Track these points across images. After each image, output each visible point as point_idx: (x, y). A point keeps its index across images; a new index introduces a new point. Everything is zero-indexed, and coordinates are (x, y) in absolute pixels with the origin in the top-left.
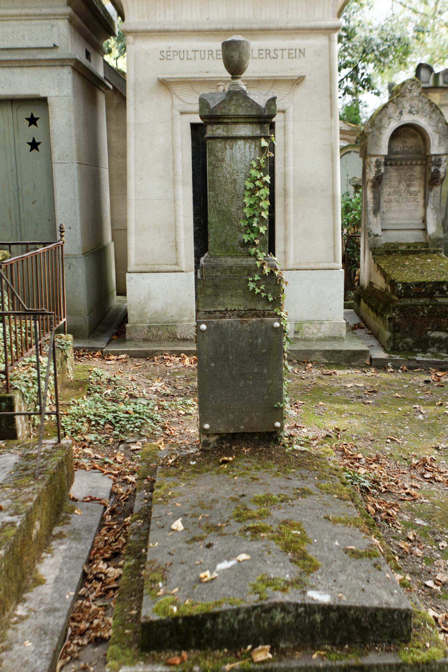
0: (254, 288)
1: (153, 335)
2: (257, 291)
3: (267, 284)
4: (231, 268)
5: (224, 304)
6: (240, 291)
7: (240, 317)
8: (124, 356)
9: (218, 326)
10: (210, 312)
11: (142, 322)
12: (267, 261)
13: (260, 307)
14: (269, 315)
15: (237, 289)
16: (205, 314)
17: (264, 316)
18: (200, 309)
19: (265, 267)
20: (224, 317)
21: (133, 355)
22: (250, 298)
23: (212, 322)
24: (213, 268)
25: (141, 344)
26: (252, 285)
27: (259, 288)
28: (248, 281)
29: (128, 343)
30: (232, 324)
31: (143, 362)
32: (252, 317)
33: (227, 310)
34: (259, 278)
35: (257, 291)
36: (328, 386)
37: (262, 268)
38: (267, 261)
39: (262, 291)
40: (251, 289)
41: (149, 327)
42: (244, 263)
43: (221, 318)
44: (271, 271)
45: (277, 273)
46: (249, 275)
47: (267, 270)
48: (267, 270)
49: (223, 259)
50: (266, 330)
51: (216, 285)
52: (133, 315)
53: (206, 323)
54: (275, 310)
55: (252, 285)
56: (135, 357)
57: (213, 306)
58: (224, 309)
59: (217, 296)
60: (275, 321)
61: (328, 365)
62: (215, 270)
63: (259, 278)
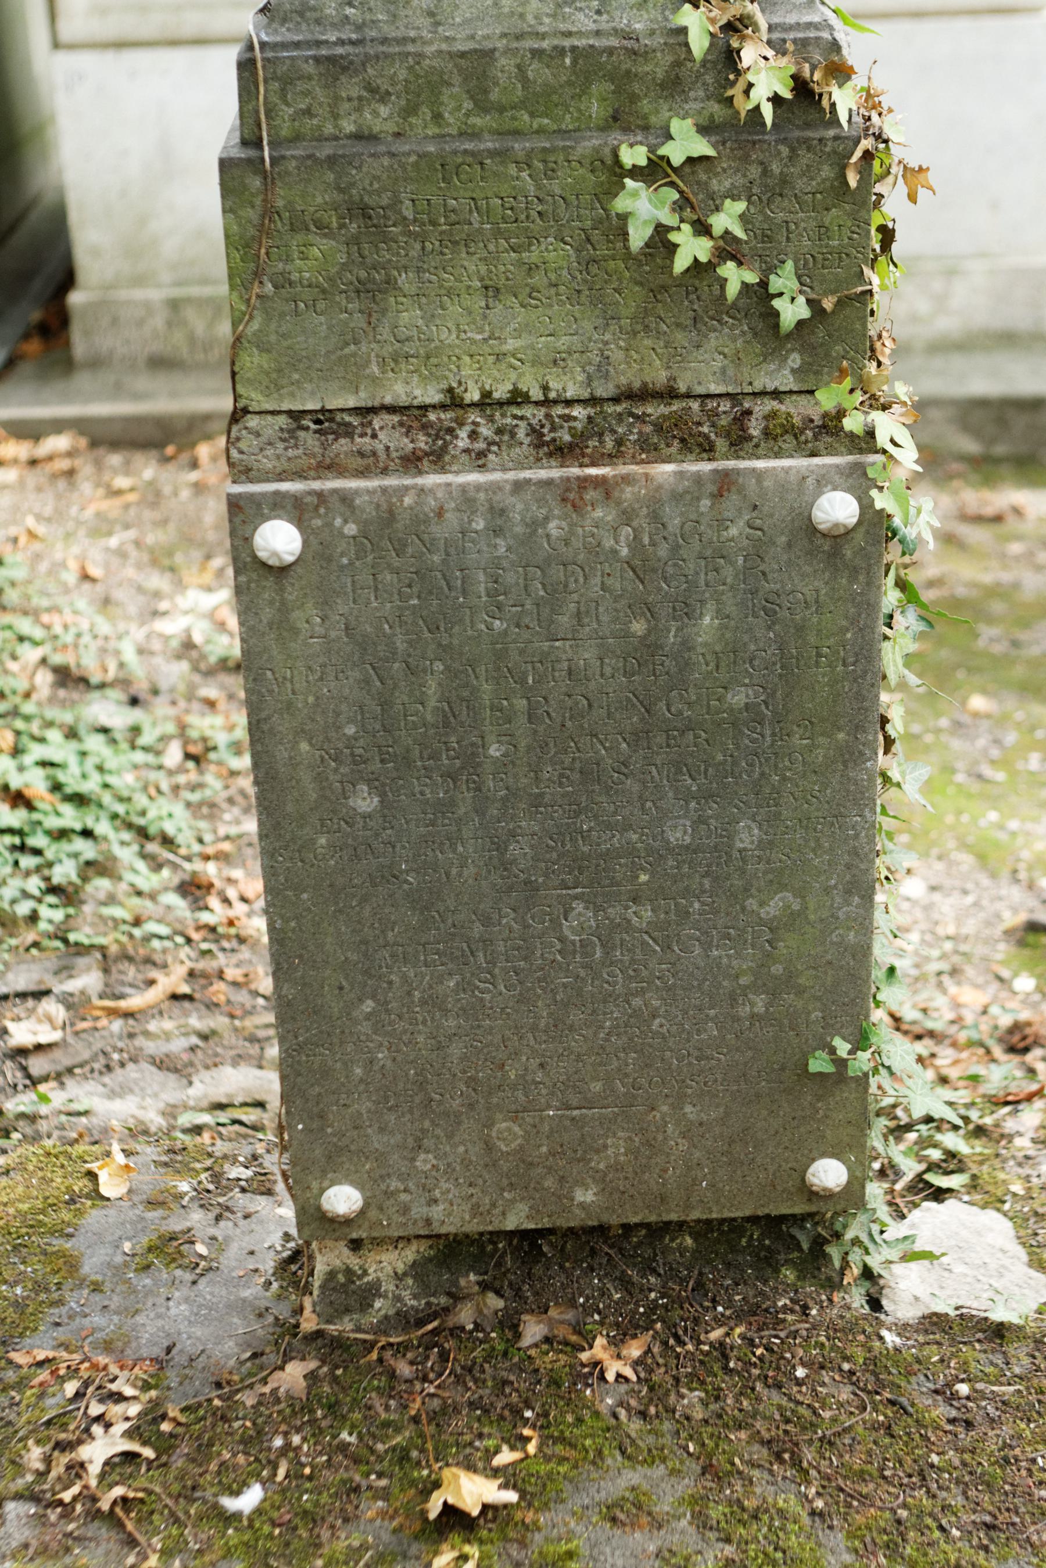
0: (661, 230)
1: (192, 339)
2: (690, 248)
3: (764, 193)
5: (430, 359)
6: (556, 254)
7: (561, 452)
8: (60, 442)
10: (325, 420)
11: (139, 281)
14: (784, 435)
15: (532, 239)
16: (289, 436)
17: (739, 440)
18: (257, 399)
19: (749, 55)
21: (106, 438)
22: (629, 302)
23: (346, 498)
24: (335, 67)
25: (142, 382)
26: (643, 207)
27: (702, 229)
29: (82, 380)
30: (497, 512)
31: (148, 469)
33: (454, 401)
34: (702, 147)
35: (690, 248)
36: (995, 591)
37: (727, 60)
39: (728, 249)
40: (638, 236)
41: (174, 305)
43: (412, 462)
44: (801, 87)
45: (844, 100)
46: (621, 120)
47: (765, 78)
48: (765, 78)
50: (757, 553)
51: (363, 211)
52: (95, 252)
53: (297, 510)
54: (827, 399)
55: (643, 207)
56: (115, 444)
57: (352, 373)
58: (432, 395)
59: (372, 291)
60: (823, 482)
61: (986, 468)
62: (351, 88)
63: (702, 147)
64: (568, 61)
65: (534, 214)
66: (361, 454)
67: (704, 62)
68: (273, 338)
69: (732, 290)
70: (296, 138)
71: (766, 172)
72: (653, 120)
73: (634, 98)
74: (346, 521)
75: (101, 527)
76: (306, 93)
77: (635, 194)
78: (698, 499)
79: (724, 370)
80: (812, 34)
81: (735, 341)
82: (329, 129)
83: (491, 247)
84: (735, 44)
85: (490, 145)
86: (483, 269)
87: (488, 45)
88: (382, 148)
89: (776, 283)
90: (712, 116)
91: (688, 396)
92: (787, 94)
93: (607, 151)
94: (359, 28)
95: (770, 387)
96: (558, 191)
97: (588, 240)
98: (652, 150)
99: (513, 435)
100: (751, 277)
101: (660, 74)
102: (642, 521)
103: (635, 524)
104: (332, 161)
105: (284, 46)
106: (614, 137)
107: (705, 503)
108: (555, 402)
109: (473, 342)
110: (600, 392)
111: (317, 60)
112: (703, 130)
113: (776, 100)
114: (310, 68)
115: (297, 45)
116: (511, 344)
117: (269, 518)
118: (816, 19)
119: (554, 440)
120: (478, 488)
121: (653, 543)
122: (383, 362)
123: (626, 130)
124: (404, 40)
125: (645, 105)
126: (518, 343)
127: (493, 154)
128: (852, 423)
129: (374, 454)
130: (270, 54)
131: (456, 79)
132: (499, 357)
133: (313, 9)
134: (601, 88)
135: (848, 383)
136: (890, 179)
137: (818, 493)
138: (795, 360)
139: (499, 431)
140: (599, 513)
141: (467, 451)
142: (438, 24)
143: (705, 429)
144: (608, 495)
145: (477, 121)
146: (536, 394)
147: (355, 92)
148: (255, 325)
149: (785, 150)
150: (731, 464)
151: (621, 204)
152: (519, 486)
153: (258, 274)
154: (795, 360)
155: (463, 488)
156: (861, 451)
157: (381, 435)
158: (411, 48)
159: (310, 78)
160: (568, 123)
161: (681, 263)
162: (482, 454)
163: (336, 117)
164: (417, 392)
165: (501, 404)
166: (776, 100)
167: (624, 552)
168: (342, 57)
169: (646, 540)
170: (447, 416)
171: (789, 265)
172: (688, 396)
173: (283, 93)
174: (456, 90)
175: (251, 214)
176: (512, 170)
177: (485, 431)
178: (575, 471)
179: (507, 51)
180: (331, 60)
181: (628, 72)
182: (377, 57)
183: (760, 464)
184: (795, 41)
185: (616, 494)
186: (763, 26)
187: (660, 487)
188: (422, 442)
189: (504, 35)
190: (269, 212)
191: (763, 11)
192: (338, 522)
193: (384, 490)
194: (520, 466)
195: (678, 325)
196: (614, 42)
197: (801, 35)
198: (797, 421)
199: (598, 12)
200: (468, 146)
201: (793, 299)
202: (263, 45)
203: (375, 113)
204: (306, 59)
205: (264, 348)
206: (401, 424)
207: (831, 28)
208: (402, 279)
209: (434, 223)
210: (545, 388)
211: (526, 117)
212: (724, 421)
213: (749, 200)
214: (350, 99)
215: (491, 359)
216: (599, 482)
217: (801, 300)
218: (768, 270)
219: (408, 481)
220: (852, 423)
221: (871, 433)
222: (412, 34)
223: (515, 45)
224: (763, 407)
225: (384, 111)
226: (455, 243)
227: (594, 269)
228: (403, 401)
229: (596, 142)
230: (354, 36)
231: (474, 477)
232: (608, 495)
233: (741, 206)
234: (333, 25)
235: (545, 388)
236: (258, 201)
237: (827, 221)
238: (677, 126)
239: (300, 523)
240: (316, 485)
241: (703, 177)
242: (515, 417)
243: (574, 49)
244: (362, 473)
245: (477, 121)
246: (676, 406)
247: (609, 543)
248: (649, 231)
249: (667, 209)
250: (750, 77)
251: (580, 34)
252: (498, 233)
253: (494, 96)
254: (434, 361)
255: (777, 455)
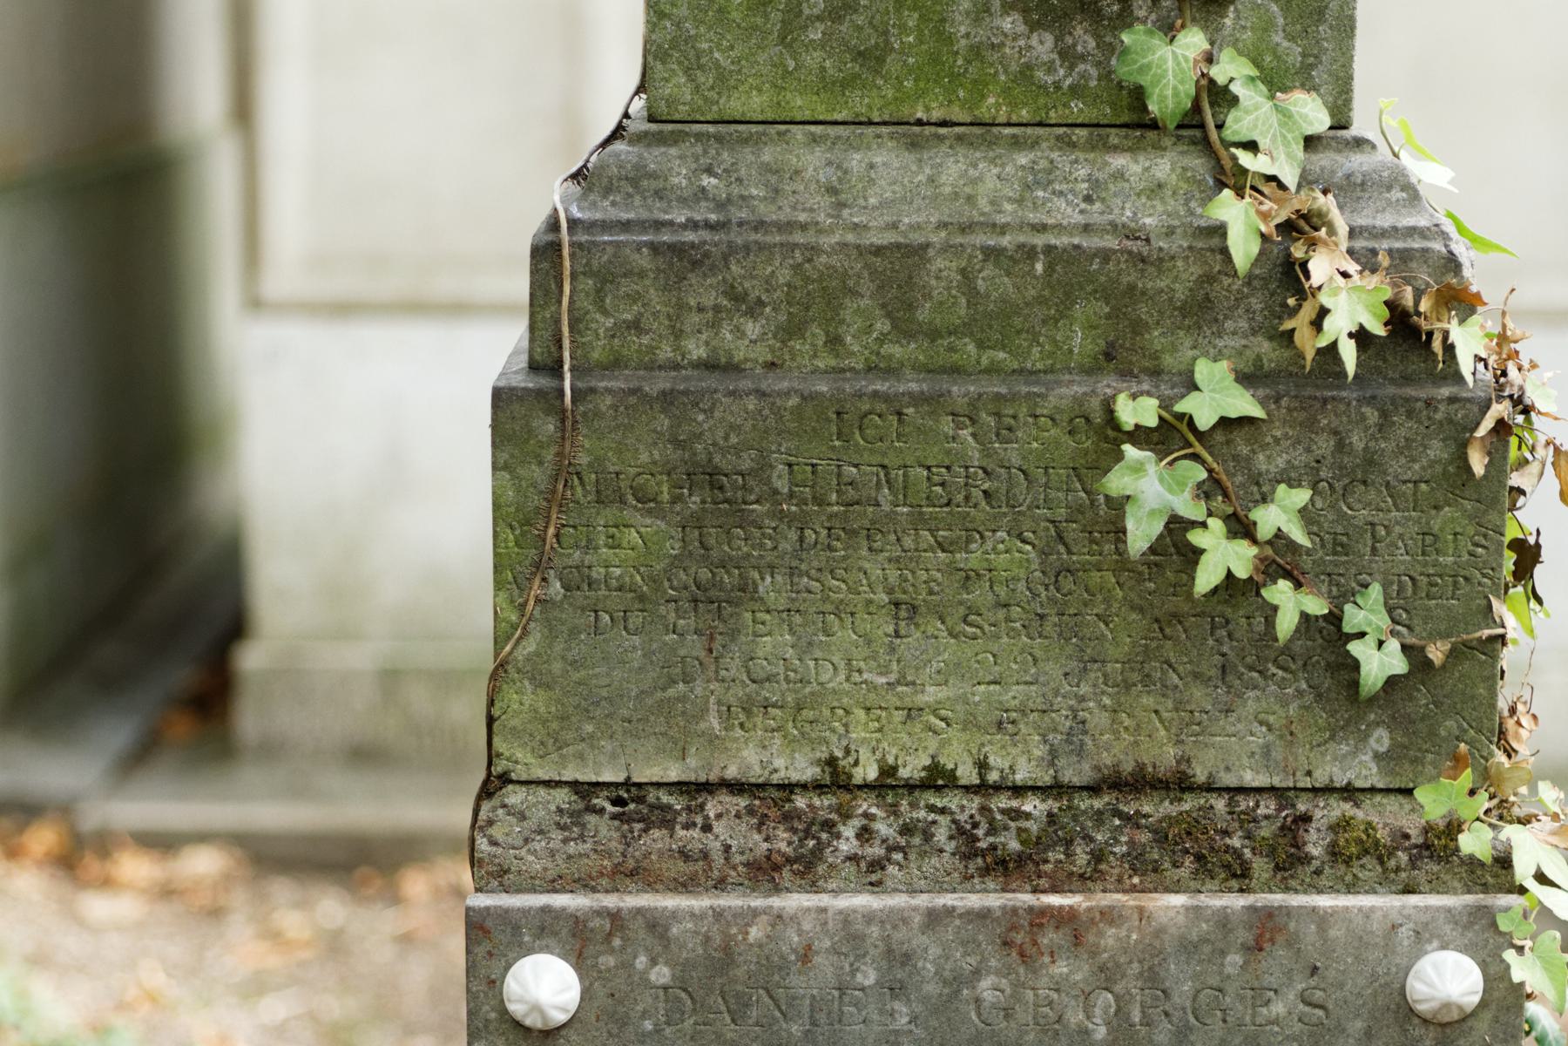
0: (1177, 526)
2: (1222, 556)
3: (1341, 478)
4: (898, 265)
5: (802, 711)
6: (1009, 557)
7: (1003, 868)
9: (722, 979)
10: (629, 798)
12: (1350, 189)
13: (1242, 747)
14: (1359, 856)
15: (973, 532)
16: (571, 822)
17: (1289, 862)
18: (523, 760)
19: (1321, 268)
20: (806, 868)
21: (273, 859)
22: (1121, 637)
23: (656, 924)
24: (681, 260)
26: (1151, 490)
27: (1241, 528)
28: (1112, 436)
29: (249, 775)
30: (899, 958)
31: (332, 907)
32: (1146, 870)
33: (836, 780)
34: (1244, 404)
35: (1222, 556)
38: (1350, 189)
39: (1281, 561)
40: (1141, 533)
42: (1066, 211)
43: (765, 872)
44: (1400, 319)
45: (1468, 342)
46: (1119, 358)
47: (1347, 304)
48: (1347, 304)
49: (812, 162)
51: (712, 478)
53: (577, 940)
54: (1435, 800)
55: (1151, 490)
57: (674, 722)
59: (718, 601)
60: (1425, 936)
62: (704, 292)
63: (1244, 404)
64: (1039, 267)
65: (977, 494)
66: (685, 855)
67: (1250, 278)
68: (557, 667)
69: (1286, 624)
70: (615, 364)
71: (1341, 446)
72: (1168, 361)
73: (1138, 327)
74: (654, 962)
75: (256, 987)
76: (634, 298)
77: (1138, 468)
78: (1223, 953)
79: (1267, 750)
80: (1417, 244)
81: (1285, 704)
82: (666, 352)
83: (908, 542)
84: (1298, 251)
85: (914, 386)
86: (893, 575)
87: (917, 238)
88: (745, 384)
89: (1354, 618)
90: (1259, 358)
91: (1209, 788)
92: (1379, 330)
93: (1095, 403)
94: (721, 206)
95: (1340, 781)
96: (1016, 460)
97: (1060, 537)
98: (1166, 404)
99: (928, 837)
100: (1317, 606)
101: (1181, 293)
102: (1130, 984)
103: (1119, 988)
104: (667, 399)
105: (605, 226)
106: (1106, 384)
107: (1234, 960)
108: (998, 788)
109: (872, 687)
110: (1070, 776)
111: (655, 248)
112: (1246, 379)
113: (1361, 336)
114: (644, 260)
115: (626, 226)
116: (931, 694)
117: (530, 951)
118: (1422, 222)
119: (993, 847)
120: (869, 917)
121: (1147, 1022)
122: (727, 713)
123: (1126, 374)
124: (789, 226)
125: (1156, 338)
126: (942, 693)
127: (917, 399)
128: (1474, 842)
129: (705, 855)
130: (584, 238)
131: (867, 286)
132: (912, 713)
133: (653, 176)
134: (1088, 309)
135: (1467, 778)
136: (1534, 468)
137: (1418, 954)
138: (1381, 739)
139: (906, 830)
140: (1061, 968)
141: (853, 858)
142: (842, 205)
143: (1236, 842)
144: (1077, 940)
145: (895, 350)
146: (967, 774)
147: (709, 299)
148: (530, 646)
149: (1372, 415)
150: (1277, 899)
151: (1117, 482)
152: (934, 918)
153: (539, 567)
154: (1381, 739)
155: (846, 917)
156: (1486, 889)
157: (718, 828)
158: (799, 238)
159: (642, 274)
160: (1035, 360)
161: (1207, 578)
162: (877, 865)
163: (678, 334)
164: (779, 763)
165: (910, 787)
166: (1361, 336)
167: (1101, 1032)
168: (693, 245)
169: (1136, 1016)
170: (823, 802)
171: (1375, 591)
172: (1209, 788)
173: (599, 295)
174: (865, 302)
175: (538, 474)
176: (947, 425)
177: (884, 828)
178: (1026, 898)
179: (946, 248)
180: (677, 250)
181: (1132, 288)
182: (747, 248)
183: (1324, 901)
184: (1390, 252)
185: (1091, 938)
186: (1342, 228)
187: (1160, 932)
188: (783, 841)
189: (942, 225)
190: (565, 472)
191: (1341, 207)
192: (641, 961)
193: (718, 914)
194: (938, 887)
195: (1196, 676)
196: (1111, 242)
197: (1398, 245)
198: (1382, 835)
199: (1088, 199)
200: (880, 386)
201: (1381, 643)
202: (573, 224)
203: (739, 332)
204: (639, 247)
205: (542, 682)
206: (751, 811)
207: (1445, 236)
208: (765, 585)
209: (820, 501)
210: (982, 766)
211: (971, 348)
212: (1266, 831)
213: (1314, 487)
214: (701, 309)
215: (899, 716)
216: (1065, 918)
217: (1393, 645)
218: (1342, 597)
219: (757, 902)
220: (1474, 842)
221: (1504, 862)
222: (803, 217)
223: (959, 240)
224: (1329, 811)
225: (752, 329)
226: (853, 533)
227: (1067, 583)
228: (756, 774)
229: (1078, 389)
230: (713, 217)
231: (863, 901)
232: (1077, 940)
233: (1302, 496)
234: (683, 201)
235: (982, 766)
236: (549, 455)
237: (1436, 525)
238: (1203, 370)
239: (579, 962)
240: (610, 901)
241: (1244, 450)
242: (932, 808)
243: (1049, 249)
244: (684, 886)
245: (895, 350)
246: (1189, 804)
247: (1075, 1017)
248: (1158, 527)
249: (1187, 494)
250: (1324, 299)
251: (1059, 228)
252: (918, 521)
253: (924, 314)
254: (808, 714)
255: (1351, 888)
